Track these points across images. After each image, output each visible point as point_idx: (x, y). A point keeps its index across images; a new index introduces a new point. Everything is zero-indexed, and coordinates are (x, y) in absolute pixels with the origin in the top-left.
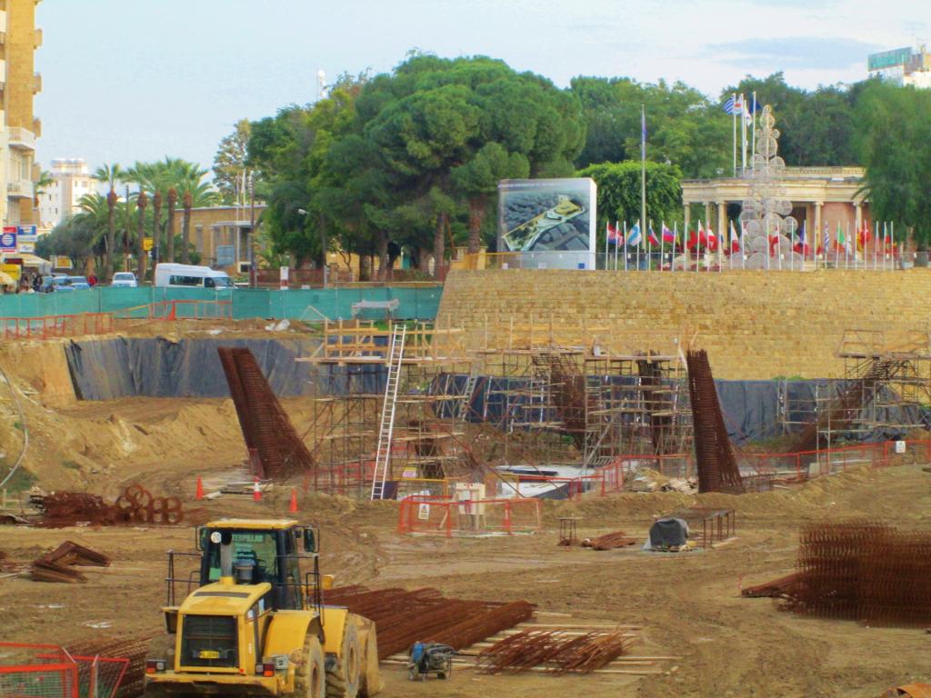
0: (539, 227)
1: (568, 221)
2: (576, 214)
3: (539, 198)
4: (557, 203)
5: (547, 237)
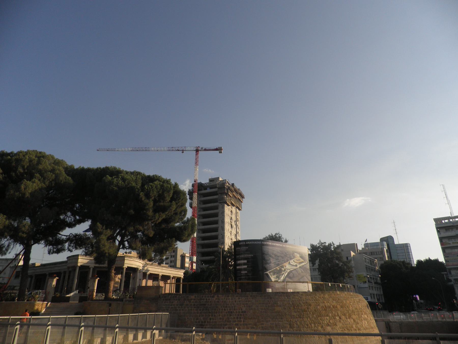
0: (287, 269)
1: (300, 267)
2: (303, 264)
3: (285, 253)
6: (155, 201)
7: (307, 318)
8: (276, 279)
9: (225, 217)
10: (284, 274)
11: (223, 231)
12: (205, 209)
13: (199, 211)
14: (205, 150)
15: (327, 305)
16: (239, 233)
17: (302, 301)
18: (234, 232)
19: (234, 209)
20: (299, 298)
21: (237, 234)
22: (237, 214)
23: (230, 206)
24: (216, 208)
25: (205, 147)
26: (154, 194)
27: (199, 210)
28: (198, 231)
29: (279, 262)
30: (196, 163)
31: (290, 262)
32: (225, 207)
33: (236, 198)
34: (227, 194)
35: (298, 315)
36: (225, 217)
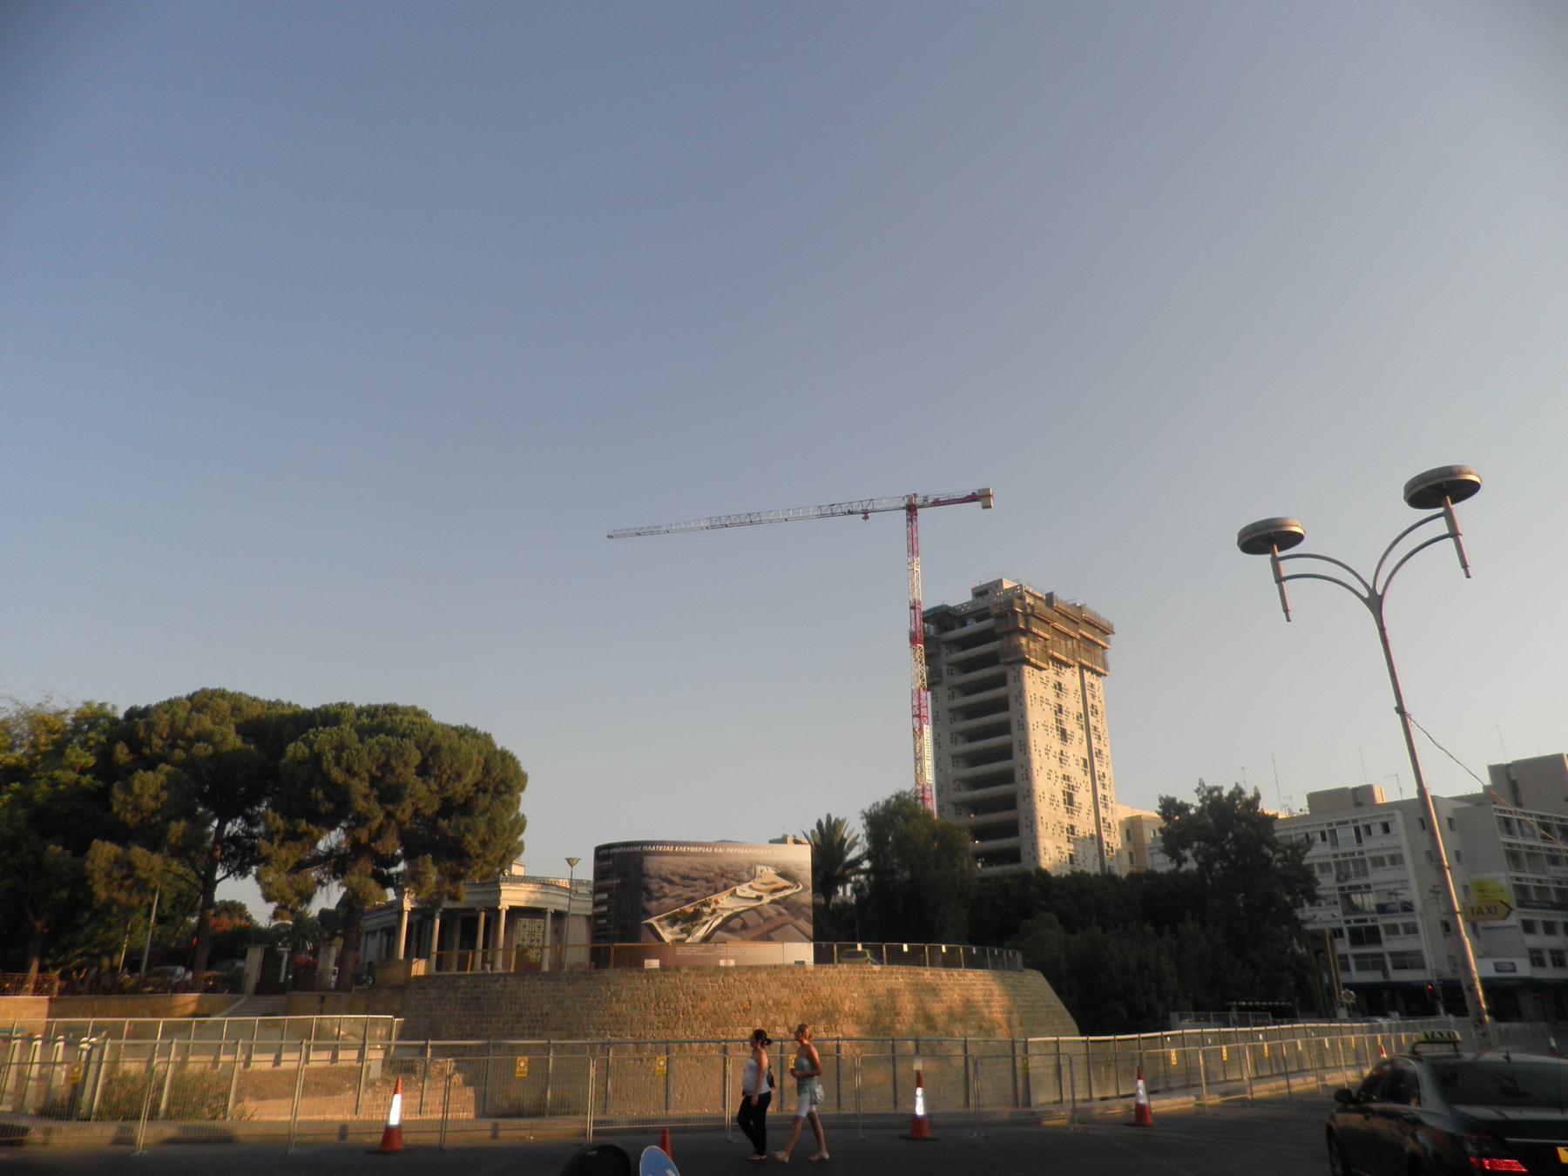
0: (722, 909)
1: (773, 902)
2: (788, 892)
3: (720, 868)
4: (754, 877)
5: (736, 923)
6: (374, 782)
7: (686, 1029)
8: (679, 937)
9: (1026, 708)
10: (710, 923)
11: (1025, 754)
12: (968, 689)
13: (949, 696)
14: (937, 503)
15: (754, 996)
16: (1106, 751)
17: (682, 990)
18: (1077, 750)
19: (1070, 678)
20: (678, 982)
21: (1095, 759)
22: (1087, 692)
23: (1045, 669)
24: (1000, 681)
25: (935, 491)
26: (367, 765)
27: (950, 693)
28: (953, 762)
29: (692, 892)
30: (913, 550)
31: (735, 890)
32: (1026, 675)
33: (1072, 638)
34: (1026, 632)
35: (663, 1023)
36: (1029, 707)
